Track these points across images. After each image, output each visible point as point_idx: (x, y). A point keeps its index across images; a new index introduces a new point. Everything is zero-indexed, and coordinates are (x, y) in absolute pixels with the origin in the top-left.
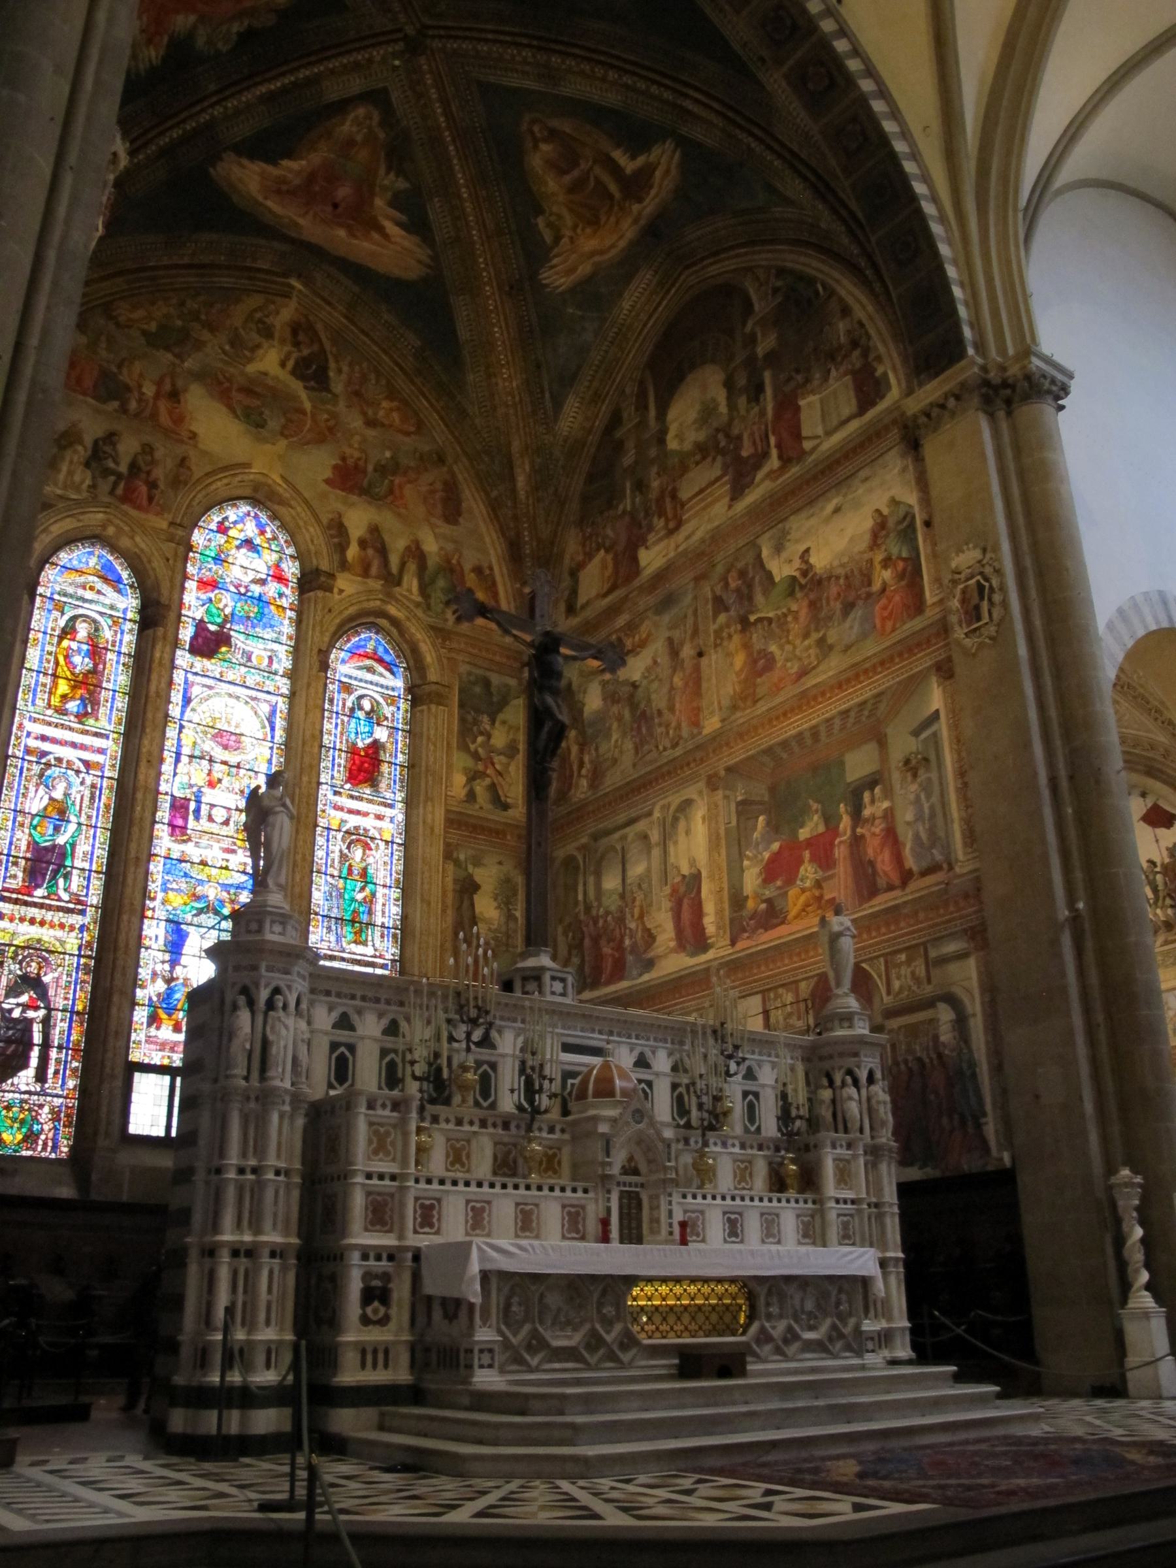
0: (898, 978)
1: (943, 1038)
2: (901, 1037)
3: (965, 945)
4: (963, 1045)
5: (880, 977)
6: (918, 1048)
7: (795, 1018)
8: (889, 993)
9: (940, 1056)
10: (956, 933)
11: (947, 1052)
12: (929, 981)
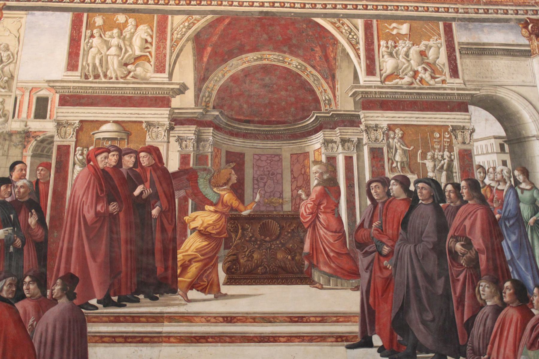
0: (391, 55)
1: (478, 160)
2: (395, 142)
3: (524, 41)
4: (521, 178)
5: (355, 46)
6: (429, 164)
7: (150, 67)
8: (370, 71)
9: (474, 185)
10: (507, 21)
11: (487, 181)
12: (454, 73)
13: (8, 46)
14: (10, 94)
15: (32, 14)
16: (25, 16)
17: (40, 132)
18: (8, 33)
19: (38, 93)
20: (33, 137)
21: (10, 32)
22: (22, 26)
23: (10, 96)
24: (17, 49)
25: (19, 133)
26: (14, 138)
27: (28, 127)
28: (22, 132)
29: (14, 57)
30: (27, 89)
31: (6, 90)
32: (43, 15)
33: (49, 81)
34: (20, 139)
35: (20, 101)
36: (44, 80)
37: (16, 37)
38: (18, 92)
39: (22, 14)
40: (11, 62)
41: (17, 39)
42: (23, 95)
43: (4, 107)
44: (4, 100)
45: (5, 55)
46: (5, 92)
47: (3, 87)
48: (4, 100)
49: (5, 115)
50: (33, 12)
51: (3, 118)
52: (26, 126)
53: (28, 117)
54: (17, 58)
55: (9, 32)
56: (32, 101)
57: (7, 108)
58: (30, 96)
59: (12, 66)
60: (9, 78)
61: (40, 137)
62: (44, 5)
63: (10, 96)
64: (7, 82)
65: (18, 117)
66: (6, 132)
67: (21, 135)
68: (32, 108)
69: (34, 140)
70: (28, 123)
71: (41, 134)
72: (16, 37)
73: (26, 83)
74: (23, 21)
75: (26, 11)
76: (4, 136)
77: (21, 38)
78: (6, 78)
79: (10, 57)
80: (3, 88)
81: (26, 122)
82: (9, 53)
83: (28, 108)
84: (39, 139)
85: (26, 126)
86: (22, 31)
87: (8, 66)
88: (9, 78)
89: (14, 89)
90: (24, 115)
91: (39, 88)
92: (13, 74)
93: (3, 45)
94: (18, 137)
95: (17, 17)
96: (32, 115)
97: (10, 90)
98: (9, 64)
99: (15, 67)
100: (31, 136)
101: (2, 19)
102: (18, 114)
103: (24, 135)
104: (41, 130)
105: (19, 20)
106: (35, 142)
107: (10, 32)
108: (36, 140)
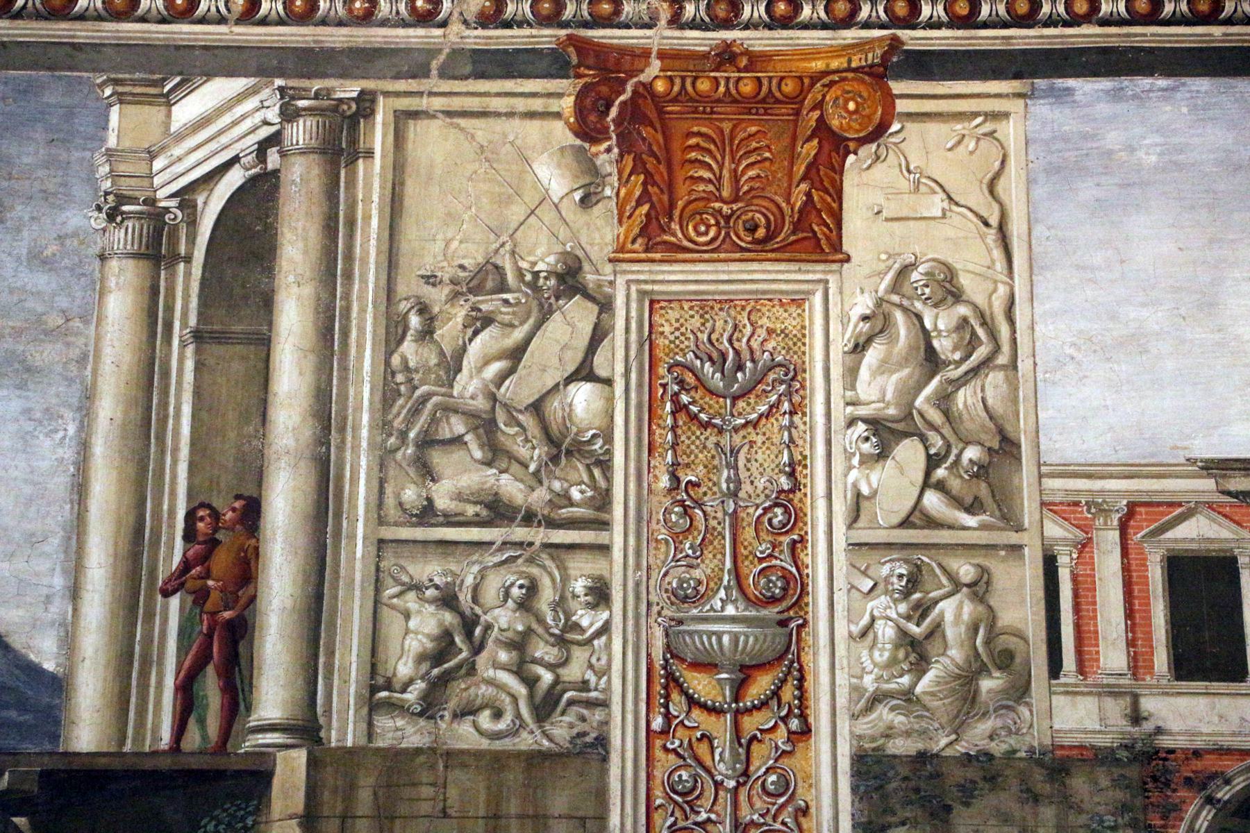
13: (951, 273)
14: (1013, 538)
15: (1051, 92)
16: (1016, 106)
17: (1223, 752)
18: (936, 205)
19: (1169, 535)
20: (1188, 781)
21: (950, 198)
22: (1012, 162)
23: (1016, 549)
24: (1002, 290)
25: (1098, 757)
26: (1079, 784)
27: (1148, 726)
28: (1123, 754)
29: (993, 336)
30: (1103, 511)
31: (984, 518)
32: (1116, 96)
33: (1217, 467)
34: (1119, 795)
35: (1075, 579)
36: (1191, 461)
37: (986, 224)
38: (1055, 530)
39: (998, 96)
40: (986, 363)
41: (992, 234)
42: (1084, 546)
43: (992, 617)
44: (983, 570)
45: (941, 326)
46: (983, 527)
47: (968, 500)
48: (983, 570)
49: (1005, 660)
50: (1060, 83)
51: (997, 674)
52: (1136, 717)
53: (1138, 663)
54: (1014, 341)
55: (942, 195)
56: (1145, 581)
57: (1008, 617)
58: (1125, 552)
59: (994, 381)
60: (990, 450)
61: (1227, 782)
62: (1114, 43)
63: (1016, 549)
64: (982, 471)
65: (1081, 669)
66: (1031, 750)
67: (1117, 771)
68: (1148, 618)
69: (1197, 801)
70: (1148, 704)
71: (1231, 766)
72: (986, 224)
73: (1089, 476)
74: (1011, 132)
75: (1017, 76)
76: (1024, 778)
77: (1017, 228)
78: (972, 453)
79: (974, 333)
80: (970, 510)
81: (1136, 698)
82: (963, 310)
83: (1129, 614)
84: (1224, 794)
85: (1136, 717)
86: (1012, 187)
87: (976, 383)
88: (990, 450)
89: (1029, 510)
90: (1113, 657)
91: (1172, 505)
92: (1009, 428)
93: (921, 269)
94: (1104, 782)
95: (975, 115)
96: (1161, 659)
97: (1010, 519)
98: (975, 371)
99: (1014, 387)
100: (1176, 778)
101: (895, 127)
102: (1079, 652)
103: (1134, 772)
104: (1227, 742)
105: (988, 127)
106: (1207, 815)
107: (950, 198)
108: (1210, 800)
